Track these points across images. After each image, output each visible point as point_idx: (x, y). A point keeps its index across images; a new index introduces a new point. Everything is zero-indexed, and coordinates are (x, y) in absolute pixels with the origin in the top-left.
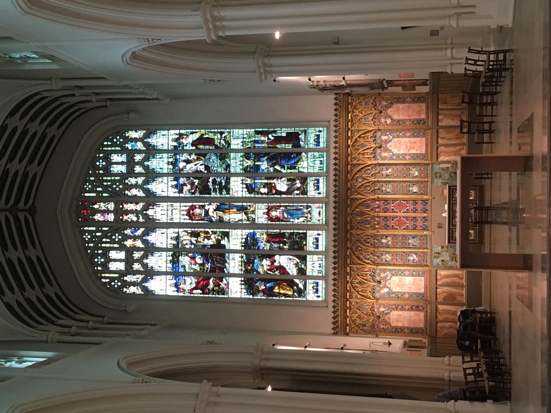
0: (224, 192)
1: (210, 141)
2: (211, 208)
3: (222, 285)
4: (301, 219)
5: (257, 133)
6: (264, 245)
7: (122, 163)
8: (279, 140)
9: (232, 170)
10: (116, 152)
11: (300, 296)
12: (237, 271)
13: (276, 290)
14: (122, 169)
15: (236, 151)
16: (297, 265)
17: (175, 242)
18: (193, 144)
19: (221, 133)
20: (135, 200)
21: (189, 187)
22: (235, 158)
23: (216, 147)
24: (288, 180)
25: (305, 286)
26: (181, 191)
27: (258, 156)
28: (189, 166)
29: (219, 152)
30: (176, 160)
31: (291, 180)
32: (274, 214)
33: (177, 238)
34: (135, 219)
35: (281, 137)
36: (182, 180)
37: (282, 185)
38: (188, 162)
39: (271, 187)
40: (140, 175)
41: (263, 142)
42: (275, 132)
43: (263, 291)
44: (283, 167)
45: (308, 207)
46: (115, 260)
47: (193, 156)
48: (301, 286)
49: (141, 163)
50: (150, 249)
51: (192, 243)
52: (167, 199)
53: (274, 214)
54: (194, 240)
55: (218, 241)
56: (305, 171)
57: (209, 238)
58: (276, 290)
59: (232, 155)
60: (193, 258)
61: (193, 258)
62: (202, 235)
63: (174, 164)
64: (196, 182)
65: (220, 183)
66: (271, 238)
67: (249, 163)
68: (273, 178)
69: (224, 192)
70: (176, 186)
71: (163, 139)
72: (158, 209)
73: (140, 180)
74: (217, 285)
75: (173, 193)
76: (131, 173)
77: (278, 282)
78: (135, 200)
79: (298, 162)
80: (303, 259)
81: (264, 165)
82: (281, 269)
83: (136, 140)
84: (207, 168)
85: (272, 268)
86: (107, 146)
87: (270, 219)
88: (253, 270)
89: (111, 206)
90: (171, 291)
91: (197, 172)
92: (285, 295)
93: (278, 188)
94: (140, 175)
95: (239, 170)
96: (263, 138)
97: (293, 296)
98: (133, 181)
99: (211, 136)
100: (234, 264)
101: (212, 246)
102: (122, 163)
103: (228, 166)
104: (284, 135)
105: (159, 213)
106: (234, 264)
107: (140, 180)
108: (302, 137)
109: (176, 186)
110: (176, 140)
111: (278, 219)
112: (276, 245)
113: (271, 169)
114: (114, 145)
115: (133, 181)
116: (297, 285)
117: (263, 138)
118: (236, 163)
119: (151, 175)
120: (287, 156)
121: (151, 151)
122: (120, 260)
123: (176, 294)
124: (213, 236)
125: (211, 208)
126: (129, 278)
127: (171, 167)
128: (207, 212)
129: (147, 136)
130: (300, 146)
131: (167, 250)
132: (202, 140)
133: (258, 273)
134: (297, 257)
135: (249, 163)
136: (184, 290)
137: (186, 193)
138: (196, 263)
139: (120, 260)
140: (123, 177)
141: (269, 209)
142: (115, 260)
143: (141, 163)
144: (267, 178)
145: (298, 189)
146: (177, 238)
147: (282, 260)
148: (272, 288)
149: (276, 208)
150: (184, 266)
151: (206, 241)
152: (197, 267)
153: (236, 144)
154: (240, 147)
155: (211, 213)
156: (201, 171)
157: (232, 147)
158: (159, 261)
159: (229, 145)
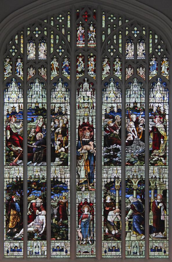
0: (107, 160)
1: (156, 145)
2: (90, 147)
3: (15, 160)
4: (80, 235)
5: (165, 192)
6: (55, 200)
7: (136, 55)
8: (157, 213)
9: (128, 168)
10: (147, 48)
11: (8, 234)
12: (30, 174)
13: (12, 212)
14: (130, 55)
15: (147, 171)
16: (37, 231)
17: (56, 110)
18: (155, 129)
19: (164, 157)
20: (98, 70)
21: (112, 125)
22: (140, 170)
23: (151, 152)
24: (118, 223)
25: (17, 239)
26: (107, 116)
27: (141, 193)
28: (132, 124)
29: (146, 154)
30: (139, 111)
31: (118, 226)
32: (86, 209)
33: (60, 113)
34: (79, 69)
35: (160, 215)
36: (118, 117)
37: (112, 217)
38: (137, 123)
39: (111, 206)
40: (124, 74)
41: (155, 198)
42: (165, 209)
43: (12, 199)
44: (131, 217)
45: (92, 241)
46: (37, 50)
47: (142, 129)
48: (17, 235)
49: (135, 74)
50: (49, 86)
51: (55, 128)
52: (100, 103)
53: (86, 209)
54: (59, 130)
55: (58, 155)
56: (127, 239)
57: (61, 146)
58: (12, 212)
59: (143, 168)
60: (41, 130)
61: (41, 130)
62: (64, 139)
63: (135, 110)
64: (117, 132)
65: (116, 156)
66: (63, 208)
67: (135, 185)
68: (120, 208)
69: (107, 160)
70: (112, 111)
71: (159, 97)
72: (89, 94)
73: (118, 74)
74: (16, 154)
75: (106, 108)
76: (126, 64)
77: (20, 213)
78: (98, 70)
79: (136, 231)
80: (43, 237)
81: (132, 199)
82: (33, 217)
83: (159, 69)
84: (130, 143)
85: (33, 208)
86: (154, 39)
87: (81, 206)
88: (31, 190)
89: (92, 44)
90: (8, 108)
91: (127, 132)
92: (8, 221)
93: (111, 213)
94: (124, 74)
95: (129, 174)
96: (159, 197)
97: (7, 228)
98: (118, 67)
99: (162, 146)
100: (36, 171)
101: (53, 149)
102: (136, 55)
103: (132, 164)
104: (162, 218)
105: (86, 95)
106: (36, 171)
107: (118, 74)
108: (160, 235)
109: (112, 111)
110: (158, 111)
111: (81, 212)
112: (55, 211)
113: (129, 206)
114: (155, 46)
115: (118, 67)
116: (18, 232)
117: (159, 197)
118: (135, 172)
119: (123, 86)
120: (141, 221)
121: (148, 86)
122: (37, 55)
123: (5, 113)
124: (63, 149)
125: (90, 147)
126: (19, 63)
127: (132, 105)
128: (87, 143)
129: (164, 82)
130: (151, 232)
131: (49, 103)
132: (158, 136)
133: (29, 195)
134: (45, 232)
135: (135, 185)
136: (9, 121)
137: (105, 121)
138: (36, 133)
139: (37, 55)
140: (122, 56)
141: (90, 205)
142: (37, 50)
143: (135, 74)
144: (120, 202)
145: (110, 232)
146: (60, 113)
147: (42, 217)
148: (14, 208)
149: (91, 211)
150: (33, 121)
151: (58, 143)
152: (32, 134)
153: (154, 171)
154: (151, 175)
155: (85, 147)
156: (127, 137)
157: (151, 168)
158: (37, 96)
159: (153, 165)
